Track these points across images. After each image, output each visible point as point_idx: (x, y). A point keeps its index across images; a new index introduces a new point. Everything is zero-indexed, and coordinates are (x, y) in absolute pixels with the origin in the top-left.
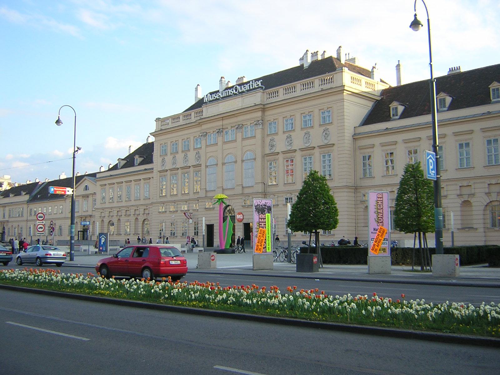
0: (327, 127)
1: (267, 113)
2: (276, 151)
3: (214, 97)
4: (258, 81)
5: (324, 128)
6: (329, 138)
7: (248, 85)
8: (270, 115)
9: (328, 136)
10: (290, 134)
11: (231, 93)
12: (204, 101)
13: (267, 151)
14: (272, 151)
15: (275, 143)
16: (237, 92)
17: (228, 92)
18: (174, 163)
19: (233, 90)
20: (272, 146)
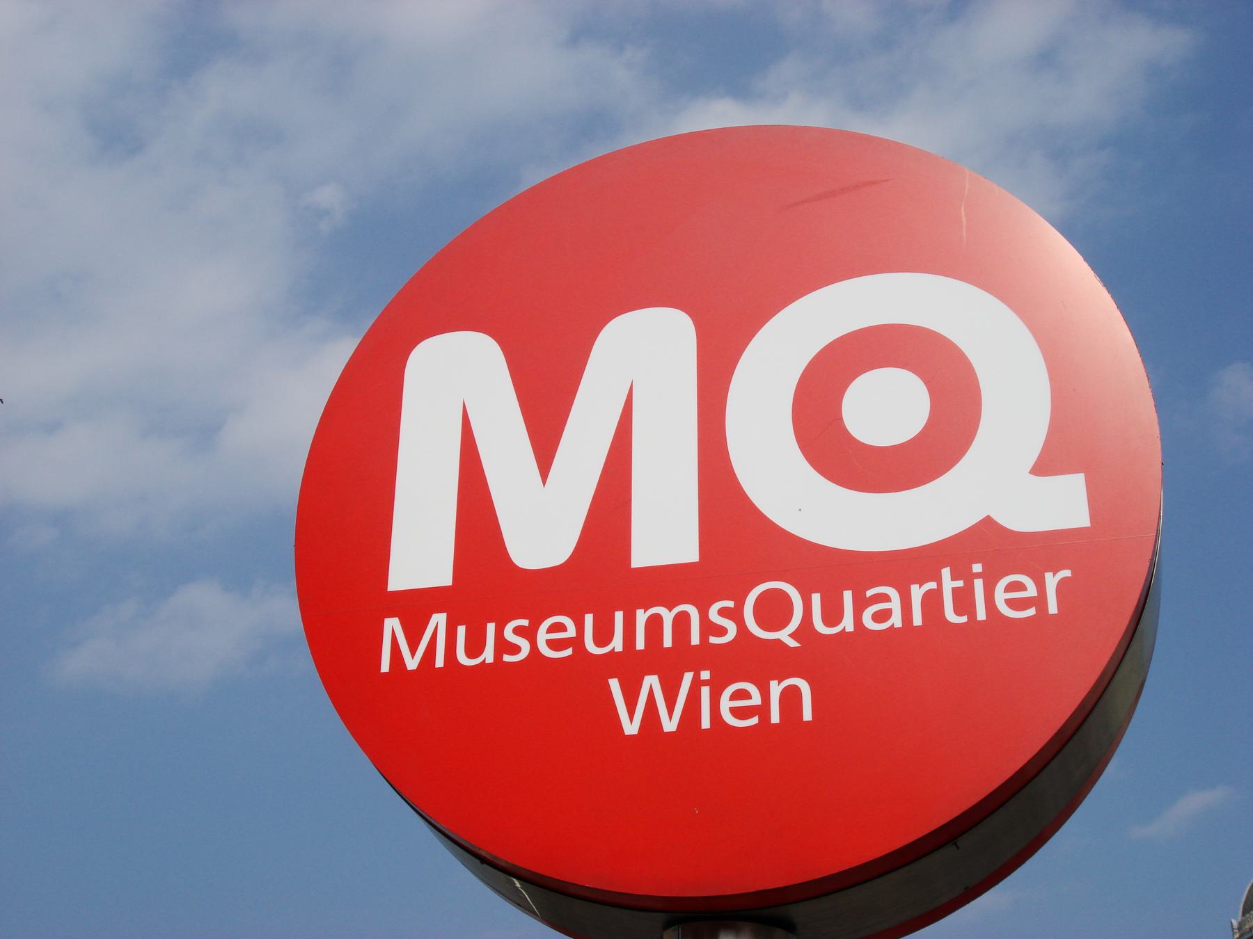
3: (503, 646)
11: (709, 628)
12: (385, 667)
16: (784, 636)
17: (682, 622)
19: (735, 614)
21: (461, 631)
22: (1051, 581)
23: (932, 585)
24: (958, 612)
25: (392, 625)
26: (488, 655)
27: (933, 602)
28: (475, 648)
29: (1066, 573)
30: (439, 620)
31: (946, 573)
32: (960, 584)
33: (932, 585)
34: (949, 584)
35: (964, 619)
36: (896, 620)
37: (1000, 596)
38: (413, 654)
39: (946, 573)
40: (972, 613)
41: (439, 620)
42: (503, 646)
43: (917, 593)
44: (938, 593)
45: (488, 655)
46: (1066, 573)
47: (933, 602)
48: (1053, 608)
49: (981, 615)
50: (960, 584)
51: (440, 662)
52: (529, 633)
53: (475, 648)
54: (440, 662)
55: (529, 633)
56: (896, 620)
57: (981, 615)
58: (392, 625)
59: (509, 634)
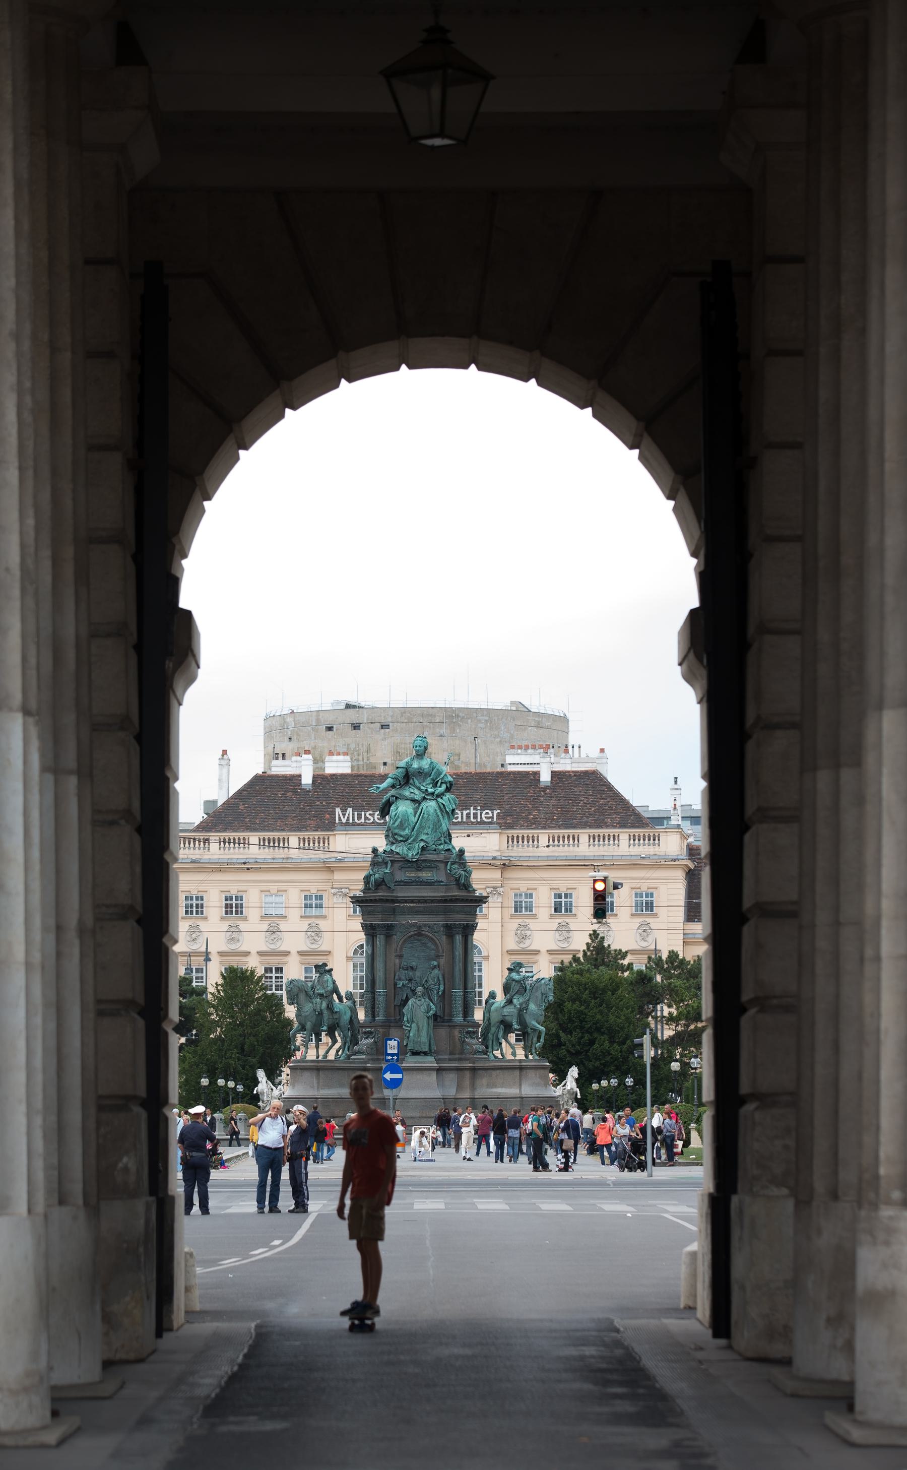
0: (646, 920)
1: (510, 874)
2: (533, 948)
3: (366, 818)
4: (492, 810)
5: (641, 920)
6: (650, 939)
7: (465, 813)
8: (521, 881)
9: (647, 936)
10: (565, 920)
12: (337, 821)
13: (512, 945)
14: (522, 945)
15: (528, 933)
18: (232, 940)
20: (524, 938)
21: (356, 813)
22: (495, 812)
23: (468, 811)
24: (474, 818)
25: (338, 811)
26: (363, 820)
27: (468, 815)
28: (359, 817)
29: (499, 811)
30: (350, 810)
31: (472, 808)
32: (475, 811)
33: (468, 811)
34: (472, 811)
35: (475, 820)
36: (460, 819)
37: (484, 815)
38: (344, 818)
39: (472, 808)
40: (476, 818)
41: (350, 810)
42: (366, 818)
43: (465, 813)
44: (470, 813)
45: (363, 820)
46: (499, 811)
47: (468, 815)
48: (495, 820)
49: (479, 820)
50: (475, 811)
51: (351, 821)
52: (373, 815)
53: (359, 817)
54: (351, 821)
55: (373, 815)
56: (460, 819)
57: (479, 820)
58: (338, 811)
59: (368, 815)
